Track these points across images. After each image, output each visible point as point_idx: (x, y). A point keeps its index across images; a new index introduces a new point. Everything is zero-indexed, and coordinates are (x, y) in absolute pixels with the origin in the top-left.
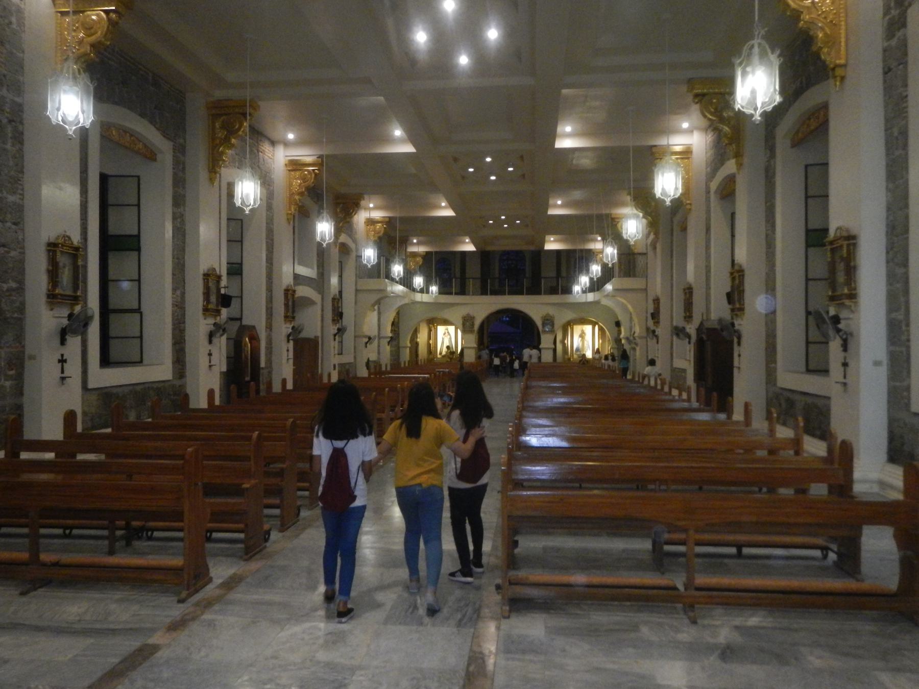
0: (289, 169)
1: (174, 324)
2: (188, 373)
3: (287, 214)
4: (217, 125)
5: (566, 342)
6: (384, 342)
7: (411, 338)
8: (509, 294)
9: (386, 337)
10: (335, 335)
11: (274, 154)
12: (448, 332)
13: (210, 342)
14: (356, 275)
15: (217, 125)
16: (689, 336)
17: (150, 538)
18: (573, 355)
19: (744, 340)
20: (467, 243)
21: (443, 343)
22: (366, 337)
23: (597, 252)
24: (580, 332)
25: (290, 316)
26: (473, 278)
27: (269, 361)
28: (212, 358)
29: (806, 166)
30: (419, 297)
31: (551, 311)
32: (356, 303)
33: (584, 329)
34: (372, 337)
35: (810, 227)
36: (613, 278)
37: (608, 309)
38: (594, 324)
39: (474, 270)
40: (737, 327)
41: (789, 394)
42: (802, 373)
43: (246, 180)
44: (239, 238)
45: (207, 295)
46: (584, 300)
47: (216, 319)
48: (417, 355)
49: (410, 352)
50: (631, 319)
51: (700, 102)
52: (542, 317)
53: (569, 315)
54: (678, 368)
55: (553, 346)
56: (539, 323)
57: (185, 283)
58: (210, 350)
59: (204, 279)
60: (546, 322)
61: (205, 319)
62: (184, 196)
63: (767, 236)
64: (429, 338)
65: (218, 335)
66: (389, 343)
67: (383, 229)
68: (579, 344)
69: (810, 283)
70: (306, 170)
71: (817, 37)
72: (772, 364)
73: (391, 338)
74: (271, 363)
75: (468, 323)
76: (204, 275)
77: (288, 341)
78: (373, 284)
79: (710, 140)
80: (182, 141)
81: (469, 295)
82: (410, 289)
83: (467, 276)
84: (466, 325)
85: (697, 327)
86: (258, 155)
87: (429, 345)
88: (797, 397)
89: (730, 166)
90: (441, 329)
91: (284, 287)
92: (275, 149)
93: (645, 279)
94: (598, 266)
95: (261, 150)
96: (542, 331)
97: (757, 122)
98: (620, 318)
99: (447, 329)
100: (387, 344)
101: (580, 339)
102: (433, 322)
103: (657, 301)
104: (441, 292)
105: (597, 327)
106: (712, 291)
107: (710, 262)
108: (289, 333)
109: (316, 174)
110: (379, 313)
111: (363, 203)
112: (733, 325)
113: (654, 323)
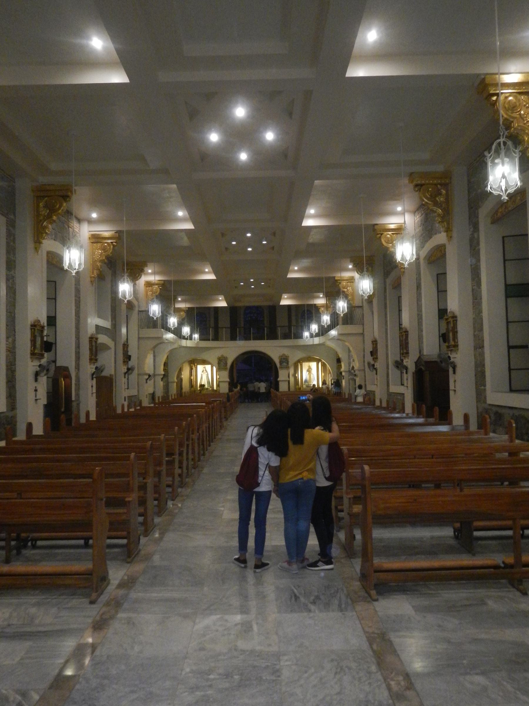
0: (92, 241)
1: (7, 366)
2: (18, 406)
3: (91, 277)
4: (41, 205)
5: (297, 375)
6: (159, 379)
7: (177, 375)
8: (253, 340)
9: (159, 375)
10: (125, 374)
11: (80, 229)
12: (206, 370)
13: (36, 380)
14: (138, 325)
15: (41, 205)
16: (406, 368)
17: (34, 547)
18: (303, 386)
19: (458, 370)
20: (220, 300)
21: (202, 378)
22: (146, 374)
23: (319, 306)
24: (307, 368)
25: (93, 359)
26: (225, 328)
27: (77, 395)
28: (38, 393)
29: (503, 237)
30: (184, 343)
31: (286, 352)
32: (138, 349)
33: (310, 365)
34: (151, 374)
35: (509, 282)
36: (337, 326)
37: (330, 348)
38: (318, 361)
39: (225, 322)
40: (452, 360)
41: (494, 409)
42: (507, 392)
43: (73, 248)
44: (54, 297)
45: (33, 341)
46: (311, 343)
47: (40, 362)
48: (181, 388)
49: (177, 385)
50: (350, 357)
51: (419, 190)
53: (300, 355)
54: (393, 393)
55: (288, 379)
56: (277, 361)
57: (15, 332)
58: (36, 387)
59: (31, 329)
61: (32, 361)
62: (15, 261)
63: (473, 290)
64: (191, 374)
65: (43, 374)
66: (162, 379)
67: (159, 290)
69: (510, 324)
70: (106, 243)
71: (524, 140)
72: (481, 387)
73: (164, 375)
74: (79, 397)
75: (222, 363)
76: (32, 326)
77: (92, 379)
78: (152, 333)
79: (418, 219)
80: (12, 217)
81: (222, 340)
82: (178, 337)
83: (220, 326)
84: (221, 363)
85: (416, 361)
86: (69, 229)
87: (191, 381)
88: (503, 411)
89: (441, 238)
90: (200, 368)
91: (89, 336)
92: (81, 225)
93: (362, 326)
94: (328, 316)
95: (70, 226)
96: (281, 368)
97: (505, 201)
98: (340, 356)
99: (205, 368)
100: (161, 380)
101: (308, 373)
102: (193, 363)
103: (375, 342)
104: (201, 339)
105: (320, 364)
106: (424, 333)
107: (421, 311)
108: (93, 372)
109: (114, 246)
110: (154, 356)
111: (145, 269)
112: (449, 357)
113: (373, 359)
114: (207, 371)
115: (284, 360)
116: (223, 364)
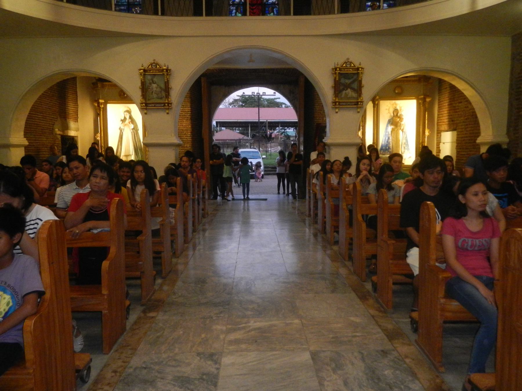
12: (131, 117)
33: (398, 108)
52: (336, 69)
60: (343, 81)
68: (389, 138)
75: (154, 86)
96: (335, 103)
99: (129, 112)
101: (390, 128)
114: (132, 121)
115: (348, 81)
116: (159, 90)
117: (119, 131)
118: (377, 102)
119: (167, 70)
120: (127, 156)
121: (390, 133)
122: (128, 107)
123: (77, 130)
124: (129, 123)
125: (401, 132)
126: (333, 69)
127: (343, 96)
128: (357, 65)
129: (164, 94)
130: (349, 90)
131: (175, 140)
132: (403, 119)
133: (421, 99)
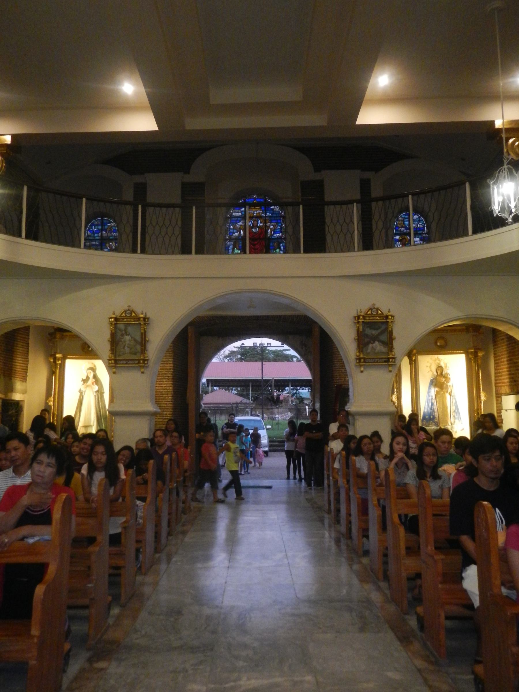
12: (95, 377)
33: (442, 364)
52: (359, 317)
60: (368, 331)
68: (432, 404)
75: (127, 338)
96: (359, 359)
101: (433, 391)
114: (97, 380)
115: (375, 332)
116: (133, 342)
117: (79, 394)
118: (414, 358)
119: (144, 319)
120: (86, 427)
121: (434, 397)
122: (93, 364)
123: (24, 392)
124: (93, 384)
125: (448, 395)
126: (355, 317)
127: (369, 351)
128: (386, 312)
129: (139, 347)
130: (377, 343)
131: (150, 407)
132: (450, 379)
133: (471, 353)
